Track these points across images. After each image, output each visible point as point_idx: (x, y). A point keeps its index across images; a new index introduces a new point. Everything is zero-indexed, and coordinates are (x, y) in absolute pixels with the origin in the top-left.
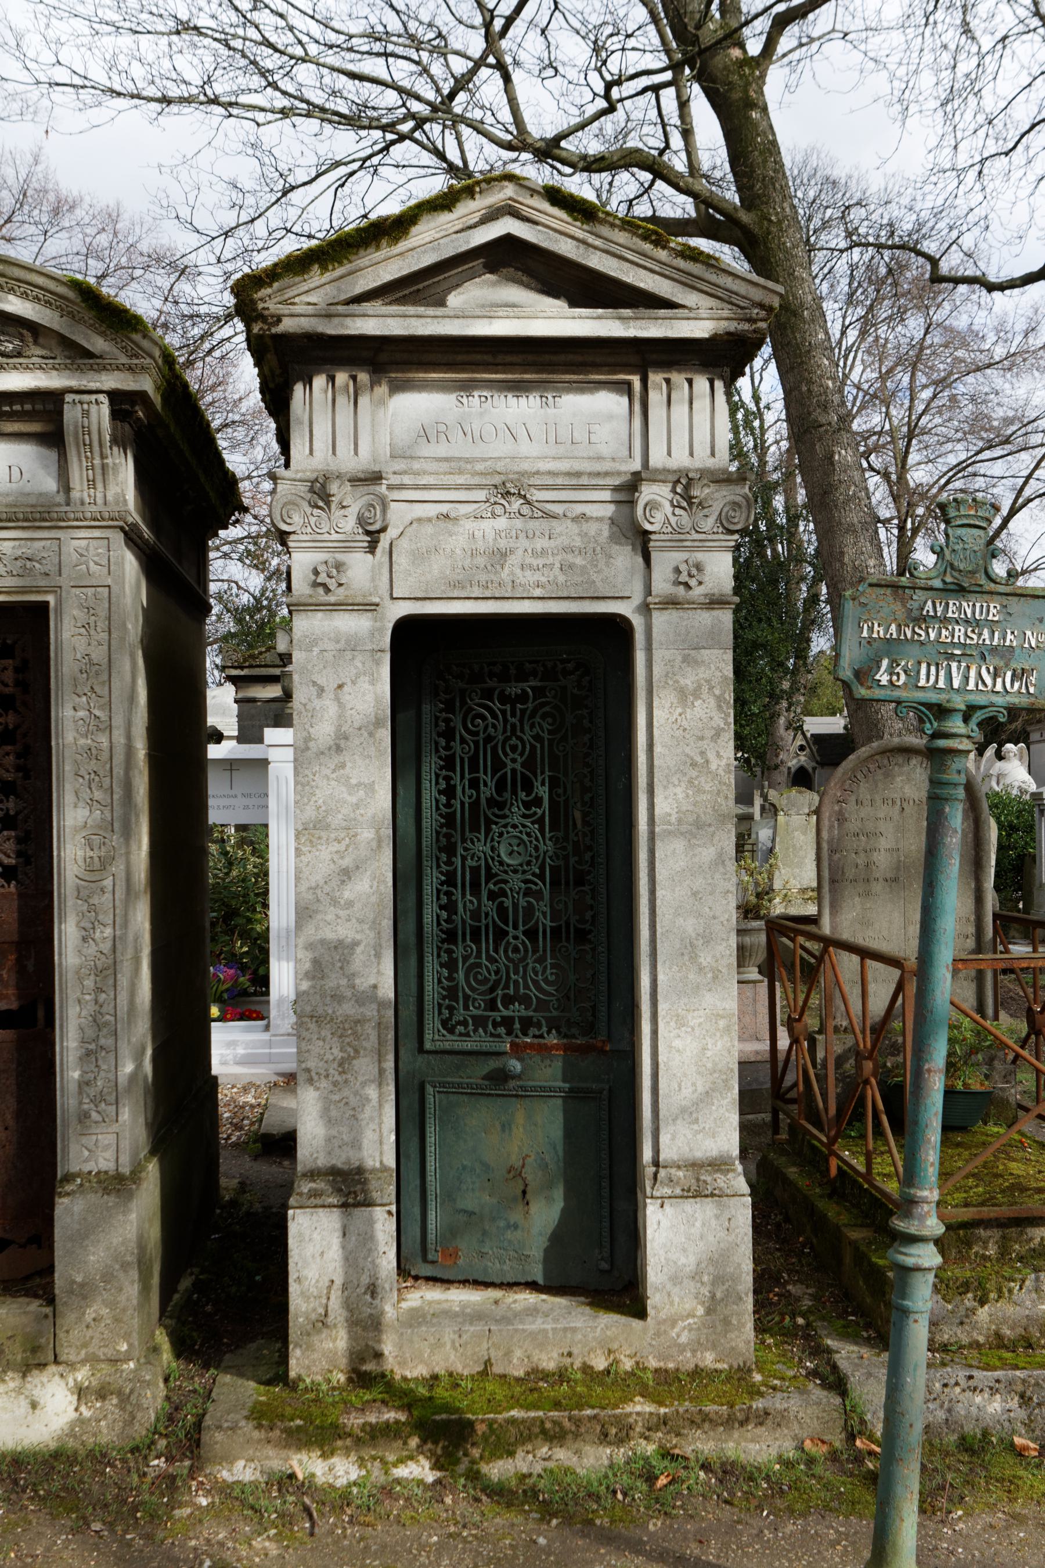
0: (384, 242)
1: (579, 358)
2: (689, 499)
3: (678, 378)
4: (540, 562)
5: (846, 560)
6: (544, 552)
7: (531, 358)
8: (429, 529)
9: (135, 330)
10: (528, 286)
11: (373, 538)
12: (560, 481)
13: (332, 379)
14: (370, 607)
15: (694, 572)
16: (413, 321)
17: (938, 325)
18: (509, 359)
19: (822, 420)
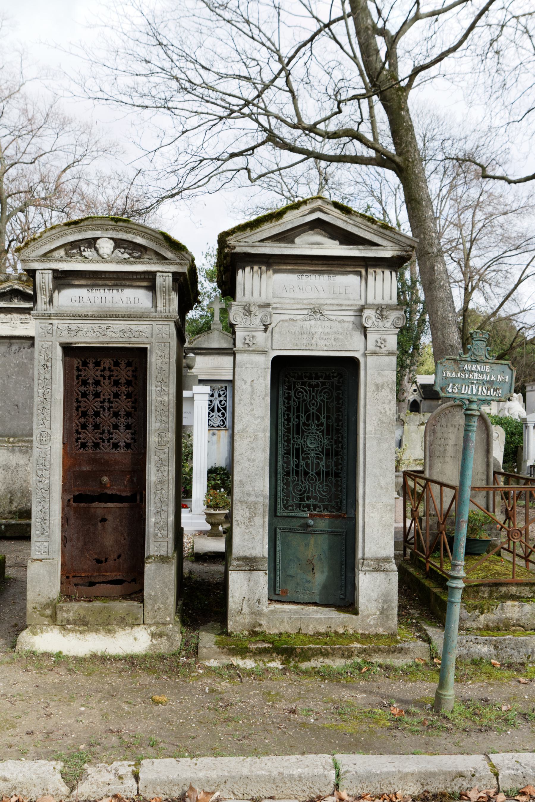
0: (274, 220)
1: (343, 263)
2: (382, 316)
3: (379, 271)
4: (327, 337)
5: (439, 313)
6: (328, 334)
7: (325, 262)
8: (286, 324)
9: (183, 251)
10: (324, 236)
11: (266, 327)
12: (335, 307)
13: (252, 268)
14: (264, 352)
15: (383, 342)
16: (284, 249)
17: (486, 192)
18: (317, 262)
19: (430, 251)
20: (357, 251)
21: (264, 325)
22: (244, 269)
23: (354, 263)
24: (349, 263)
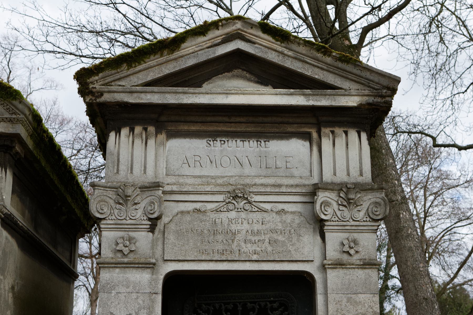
0: (165, 52)
1: (280, 119)
2: (349, 200)
3: (339, 131)
4: (257, 238)
5: (409, 264)
6: (259, 233)
7: (251, 119)
8: (188, 218)
9: (15, 99)
10: (249, 80)
11: (153, 223)
12: (268, 190)
13: (132, 130)
14: (150, 266)
15: (352, 245)
16: (181, 96)
17: (435, 168)
18: (238, 119)
19: (394, 198)
20: (302, 97)
21: (150, 219)
22: (118, 132)
23: (299, 120)
24: (291, 120)
